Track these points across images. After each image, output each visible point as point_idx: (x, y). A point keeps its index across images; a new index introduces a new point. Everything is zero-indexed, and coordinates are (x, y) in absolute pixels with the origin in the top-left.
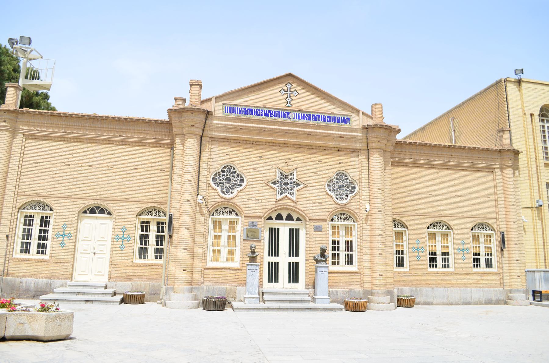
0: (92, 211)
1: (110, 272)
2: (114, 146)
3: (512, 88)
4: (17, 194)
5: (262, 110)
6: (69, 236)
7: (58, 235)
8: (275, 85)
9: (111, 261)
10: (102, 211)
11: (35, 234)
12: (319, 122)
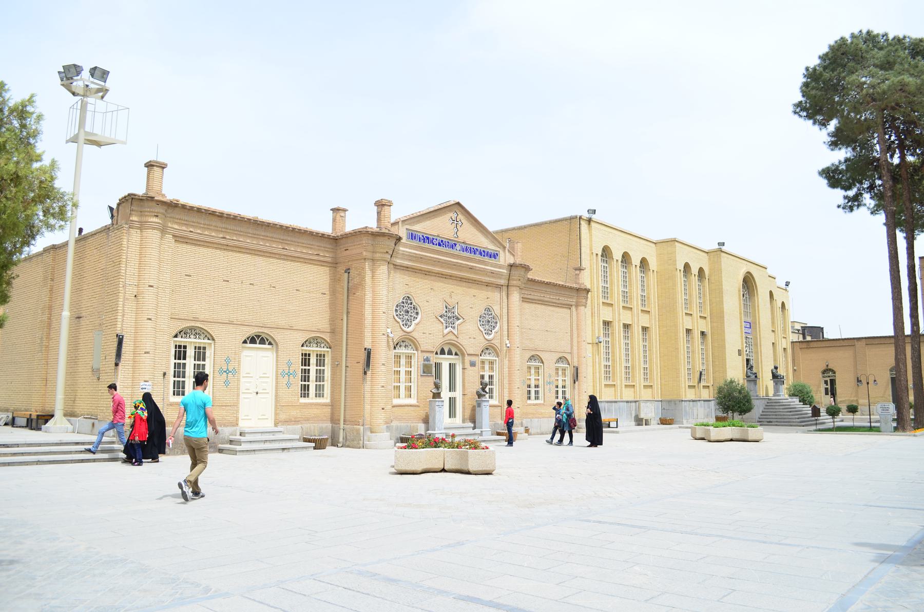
0: (253, 341)
1: (276, 414)
2: (275, 261)
3: (584, 225)
6: (230, 371)
8: (445, 213)
10: (262, 342)
11: (313, 375)
12: (478, 257)
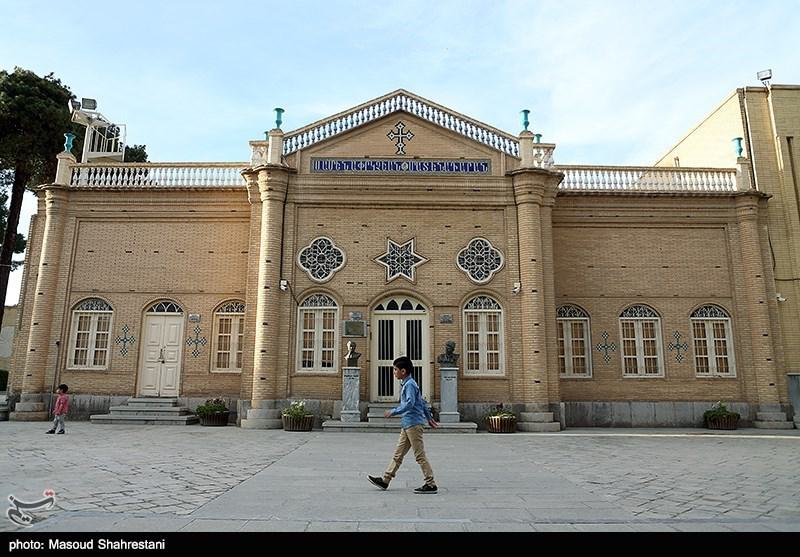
1: (181, 385)
4: (70, 291)
5: (364, 163)
7: (117, 340)
9: (182, 372)
10: (171, 309)
